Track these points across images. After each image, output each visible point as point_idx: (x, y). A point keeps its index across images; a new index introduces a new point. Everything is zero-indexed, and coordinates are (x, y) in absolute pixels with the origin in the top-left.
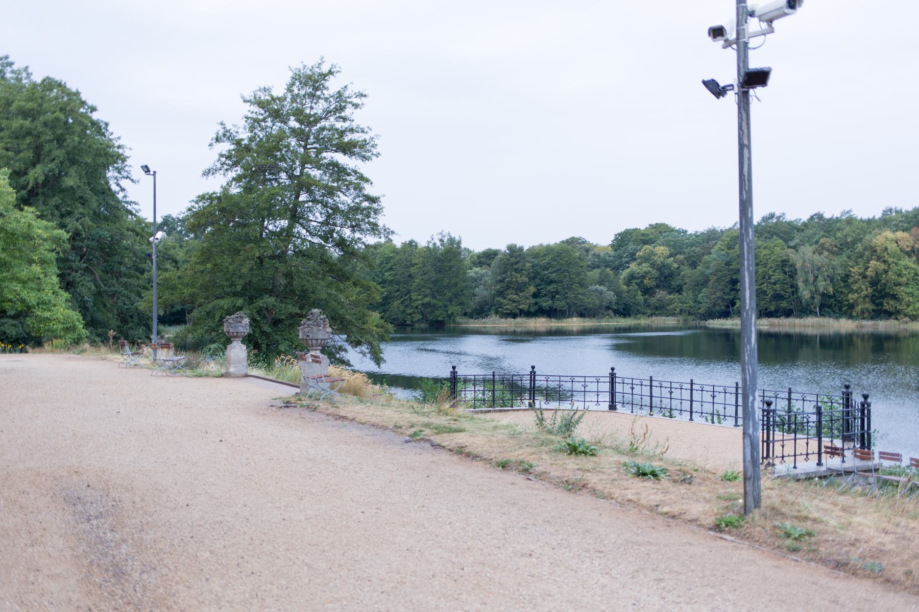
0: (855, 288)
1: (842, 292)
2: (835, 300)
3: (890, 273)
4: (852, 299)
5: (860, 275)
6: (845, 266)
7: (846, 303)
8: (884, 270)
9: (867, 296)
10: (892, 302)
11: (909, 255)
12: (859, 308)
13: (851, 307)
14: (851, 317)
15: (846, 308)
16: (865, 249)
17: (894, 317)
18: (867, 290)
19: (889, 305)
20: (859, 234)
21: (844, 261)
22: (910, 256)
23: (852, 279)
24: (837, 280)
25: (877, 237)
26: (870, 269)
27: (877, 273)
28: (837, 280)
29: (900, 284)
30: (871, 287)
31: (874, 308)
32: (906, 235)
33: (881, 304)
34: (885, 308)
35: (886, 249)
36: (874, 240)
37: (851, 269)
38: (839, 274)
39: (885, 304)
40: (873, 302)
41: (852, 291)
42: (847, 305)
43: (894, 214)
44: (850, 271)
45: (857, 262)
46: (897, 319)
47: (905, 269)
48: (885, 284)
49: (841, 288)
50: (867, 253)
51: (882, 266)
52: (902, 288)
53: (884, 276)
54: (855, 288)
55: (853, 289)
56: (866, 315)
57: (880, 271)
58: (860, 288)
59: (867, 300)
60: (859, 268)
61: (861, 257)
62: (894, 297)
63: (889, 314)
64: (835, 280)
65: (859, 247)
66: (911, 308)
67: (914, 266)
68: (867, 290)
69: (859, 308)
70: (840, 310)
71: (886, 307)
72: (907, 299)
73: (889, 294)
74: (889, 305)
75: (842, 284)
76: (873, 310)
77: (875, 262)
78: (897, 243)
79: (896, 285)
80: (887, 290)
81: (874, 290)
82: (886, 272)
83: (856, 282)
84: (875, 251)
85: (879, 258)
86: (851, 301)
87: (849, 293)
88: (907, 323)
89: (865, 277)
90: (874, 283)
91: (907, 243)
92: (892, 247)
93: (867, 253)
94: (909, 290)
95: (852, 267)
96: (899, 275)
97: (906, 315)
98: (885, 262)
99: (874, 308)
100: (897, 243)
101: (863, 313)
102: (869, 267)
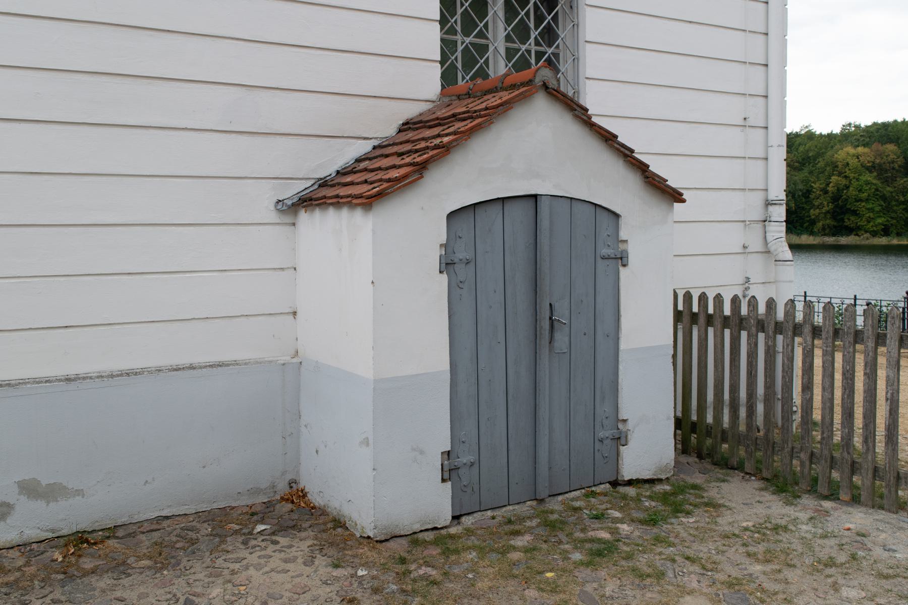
0: (816, 204)
1: (803, 207)
2: (797, 217)
3: (851, 189)
4: (814, 215)
5: (821, 191)
6: (806, 181)
7: (808, 219)
8: (845, 185)
9: (828, 212)
10: (852, 218)
11: (870, 169)
12: (821, 224)
13: (813, 223)
14: (812, 233)
15: (807, 224)
16: (827, 165)
17: (854, 233)
18: (828, 206)
19: (851, 220)
20: (821, 149)
21: (806, 177)
22: (871, 172)
23: (814, 194)
24: (799, 196)
25: (839, 153)
26: (831, 185)
27: (838, 190)
28: (799, 196)
29: (861, 200)
30: (832, 203)
31: (835, 224)
32: (866, 150)
33: (843, 220)
34: (846, 224)
35: (848, 164)
36: (836, 156)
37: (813, 184)
38: (800, 190)
39: (846, 220)
40: (834, 218)
41: (813, 206)
42: (808, 221)
43: (853, 129)
44: (812, 187)
45: (818, 178)
46: (857, 235)
47: (866, 184)
48: (846, 200)
49: (802, 203)
50: (828, 169)
51: (844, 182)
52: (863, 204)
53: (845, 191)
54: (816, 204)
55: (814, 205)
56: (827, 232)
57: (841, 187)
58: (821, 203)
59: (829, 216)
60: (821, 184)
61: (823, 172)
62: (855, 213)
63: (849, 231)
64: (796, 196)
65: (821, 164)
66: (871, 224)
67: (874, 182)
68: (828, 206)
69: (821, 224)
70: (802, 226)
71: (847, 223)
72: (867, 215)
73: (849, 209)
74: (851, 220)
75: (804, 200)
76: (835, 227)
77: (836, 178)
78: (858, 158)
79: (857, 201)
80: (848, 206)
81: (836, 206)
82: (847, 187)
83: (818, 198)
84: (837, 166)
85: (840, 174)
86: (813, 217)
87: (810, 209)
88: (867, 239)
89: (826, 192)
90: (836, 198)
91: (868, 159)
92: (853, 162)
93: (828, 169)
94: (870, 206)
95: (813, 183)
96: (860, 191)
97: (866, 232)
98: (846, 177)
99: (835, 224)
100: (858, 158)
101: (824, 229)
102: (831, 182)
